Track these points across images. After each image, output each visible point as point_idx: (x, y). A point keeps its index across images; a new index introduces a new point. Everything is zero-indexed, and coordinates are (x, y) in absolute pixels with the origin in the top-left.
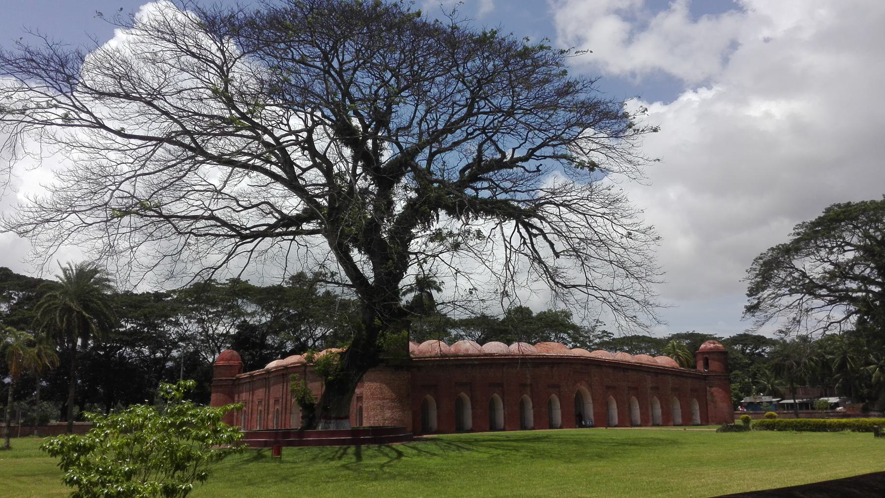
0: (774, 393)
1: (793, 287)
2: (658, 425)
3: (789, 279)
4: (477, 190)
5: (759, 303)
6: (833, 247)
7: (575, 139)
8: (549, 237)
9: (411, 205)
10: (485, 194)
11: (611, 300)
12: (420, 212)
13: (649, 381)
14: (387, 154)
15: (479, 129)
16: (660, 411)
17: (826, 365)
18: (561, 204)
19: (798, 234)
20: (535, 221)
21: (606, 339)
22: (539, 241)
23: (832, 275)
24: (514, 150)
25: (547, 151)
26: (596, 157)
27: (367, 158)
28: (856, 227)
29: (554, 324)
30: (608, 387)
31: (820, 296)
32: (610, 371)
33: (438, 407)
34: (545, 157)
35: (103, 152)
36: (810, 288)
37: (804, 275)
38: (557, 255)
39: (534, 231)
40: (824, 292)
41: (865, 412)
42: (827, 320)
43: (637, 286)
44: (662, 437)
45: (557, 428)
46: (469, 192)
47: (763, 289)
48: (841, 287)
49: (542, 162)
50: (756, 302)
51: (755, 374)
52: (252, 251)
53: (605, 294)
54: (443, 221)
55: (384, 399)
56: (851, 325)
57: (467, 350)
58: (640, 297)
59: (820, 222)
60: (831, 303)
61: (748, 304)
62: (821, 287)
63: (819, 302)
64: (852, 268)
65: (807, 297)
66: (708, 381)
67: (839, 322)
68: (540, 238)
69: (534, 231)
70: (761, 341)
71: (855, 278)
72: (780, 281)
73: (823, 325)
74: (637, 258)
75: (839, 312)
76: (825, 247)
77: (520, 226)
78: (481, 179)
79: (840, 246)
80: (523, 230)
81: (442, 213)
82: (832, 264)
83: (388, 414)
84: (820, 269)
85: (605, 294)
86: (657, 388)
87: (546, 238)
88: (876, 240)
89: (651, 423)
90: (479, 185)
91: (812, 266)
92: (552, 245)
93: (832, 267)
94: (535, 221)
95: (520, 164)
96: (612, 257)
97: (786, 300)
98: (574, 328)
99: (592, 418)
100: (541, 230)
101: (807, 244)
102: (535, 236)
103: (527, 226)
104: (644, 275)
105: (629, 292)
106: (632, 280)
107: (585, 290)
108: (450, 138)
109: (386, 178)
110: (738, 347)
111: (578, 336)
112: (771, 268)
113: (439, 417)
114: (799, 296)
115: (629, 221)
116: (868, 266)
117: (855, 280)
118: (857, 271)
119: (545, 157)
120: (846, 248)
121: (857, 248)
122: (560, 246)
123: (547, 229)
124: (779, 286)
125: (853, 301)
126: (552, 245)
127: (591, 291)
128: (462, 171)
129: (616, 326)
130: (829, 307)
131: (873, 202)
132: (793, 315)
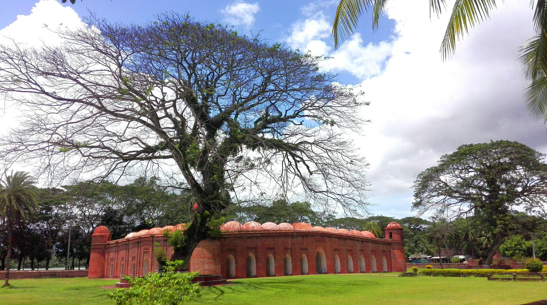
0: (428, 253)
1: (440, 192)
2: (363, 272)
3: (437, 187)
4: (263, 133)
5: (421, 201)
6: (463, 169)
7: (323, 106)
8: (307, 162)
9: (226, 141)
10: (268, 136)
11: (342, 200)
12: (231, 146)
13: (359, 245)
14: (213, 113)
15: (266, 98)
16: (365, 264)
17: (457, 236)
18: (313, 143)
19: (443, 161)
20: (298, 153)
21: (331, 220)
22: (301, 165)
23: (462, 185)
24: (287, 111)
25: (306, 112)
26: (335, 118)
27: (201, 113)
28: (475, 158)
29: (302, 210)
30: (335, 250)
31: (455, 197)
32: (337, 240)
33: (236, 263)
34: (304, 116)
35: (40, 106)
36: (449, 192)
37: (446, 185)
38: (311, 173)
39: (298, 159)
40: (457, 195)
41: (481, 265)
42: (459, 210)
43: (356, 193)
44: (369, 280)
45: (305, 274)
46: (260, 135)
47: (423, 192)
48: (467, 192)
49: (302, 119)
50: (419, 200)
51: (416, 241)
52: (125, 167)
53: (339, 197)
54: (246, 152)
55: (204, 257)
56: (471, 214)
57: (253, 227)
58: (358, 199)
59: (455, 155)
60: (461, 201)
61: (415, 201)
62: (456, 192)
63: (454, 201)
64: (473, 181)
65: (448, 197)
66: (390, 245)
67: (466, 212)
68: (301, 163)
69: (298, 159)
70: (419, 221)
71: (475, 187)
72: (433, 188)
73: (456, 214)
74: (356, 176)
75: (466, 207)
76: (458, 169)
77: (288, 154)
78: (267, 127)
79: (465, 169)
80: (290, 158)
81: (244, 146)
82: (462, 178)
83: (207, 267)
84: (455, 182)
85: (339, 197)
86: (363, 250)
87: (304, 163)
88: (487, 166)
89: (359, 271)
90: (264, 131)
91: (449, 179)
92: (308, 167)
93: (461, 180)
94: (298, 153)
95: (290, 119)
96: (342, 175)
97: (435, 199)
98: (312, 212)
99: (326, 268)
100: (302, 159)
101: (448, 167)
102: (299, 162)
103: (294, 156)
104: (360, 186)
105: (352, 196)
106: (353, 188)
107: (326, 194)
108: (251, 103)
109: (213, 127)
110: (407, 225)
111: (315, 218)
112: (427, 181)
113: (236, 269)
114: (443, 197)
115: (352, 154)
116: (482, 180)
117: (475, 188)
118: (476, 183)
119: (304, 116)
120: (470, 170)
121: (476, 170)
122: (313, 167)
123: (305, 158)
124: (432, 191)
125: (473, 200)
126: (308, 167)
127: (329, 195)
128: (256, 123)
129: (340, 213)
130: (460, 204)
131: (485, 144)
132: (440, 208)
